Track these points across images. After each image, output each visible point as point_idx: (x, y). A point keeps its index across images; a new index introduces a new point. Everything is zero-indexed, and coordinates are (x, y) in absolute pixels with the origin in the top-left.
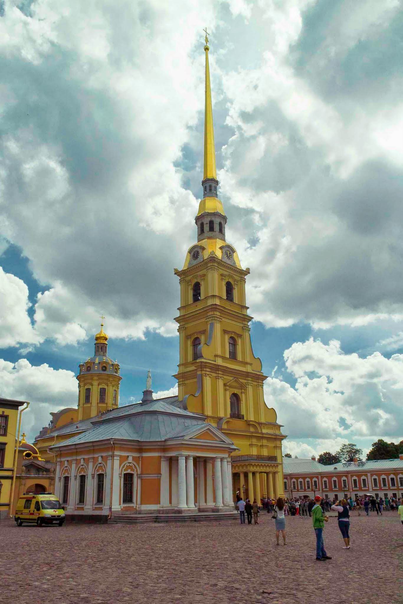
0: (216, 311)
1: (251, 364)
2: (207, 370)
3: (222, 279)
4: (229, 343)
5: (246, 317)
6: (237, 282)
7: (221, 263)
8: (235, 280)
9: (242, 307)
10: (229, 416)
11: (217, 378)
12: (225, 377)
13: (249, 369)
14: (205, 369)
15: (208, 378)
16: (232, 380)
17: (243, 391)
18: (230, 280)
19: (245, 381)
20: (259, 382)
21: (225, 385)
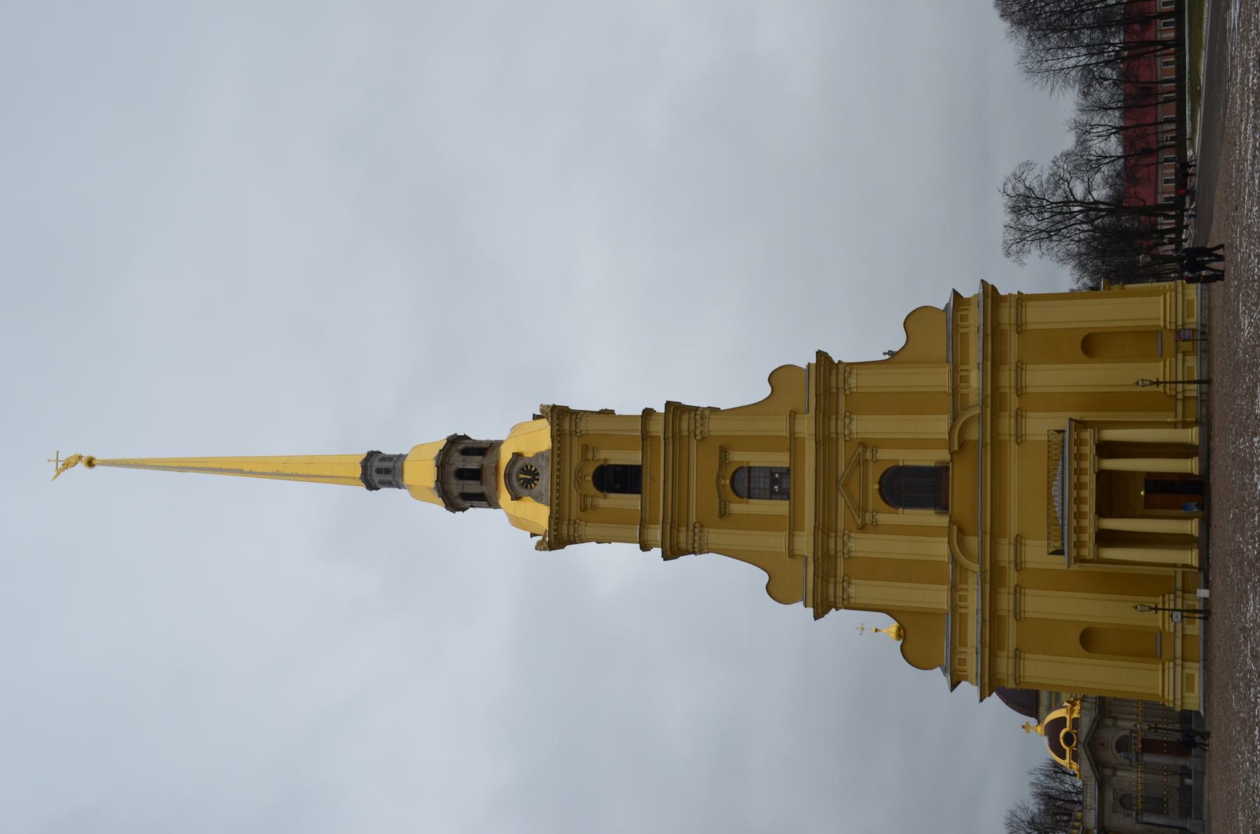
0: (678, 543)
1: (793, 415)
2: (831, 592)
3: (594, 508)
4: (749, 497)
5: (670, 435)
6: (585, 448)
7: (557, 512)
8: (585, 460)
9: (647, 437)
10: (943, 521)
11: (849, 558)
12: (841, 526)
13: (806, 427)
14: (832, 599)
15: (852, 590)
16: (845, 501)
17: (869, 456)
18: (589, 478)
19: (842, 443)
20: (837, 389)
21: (863, 528)
